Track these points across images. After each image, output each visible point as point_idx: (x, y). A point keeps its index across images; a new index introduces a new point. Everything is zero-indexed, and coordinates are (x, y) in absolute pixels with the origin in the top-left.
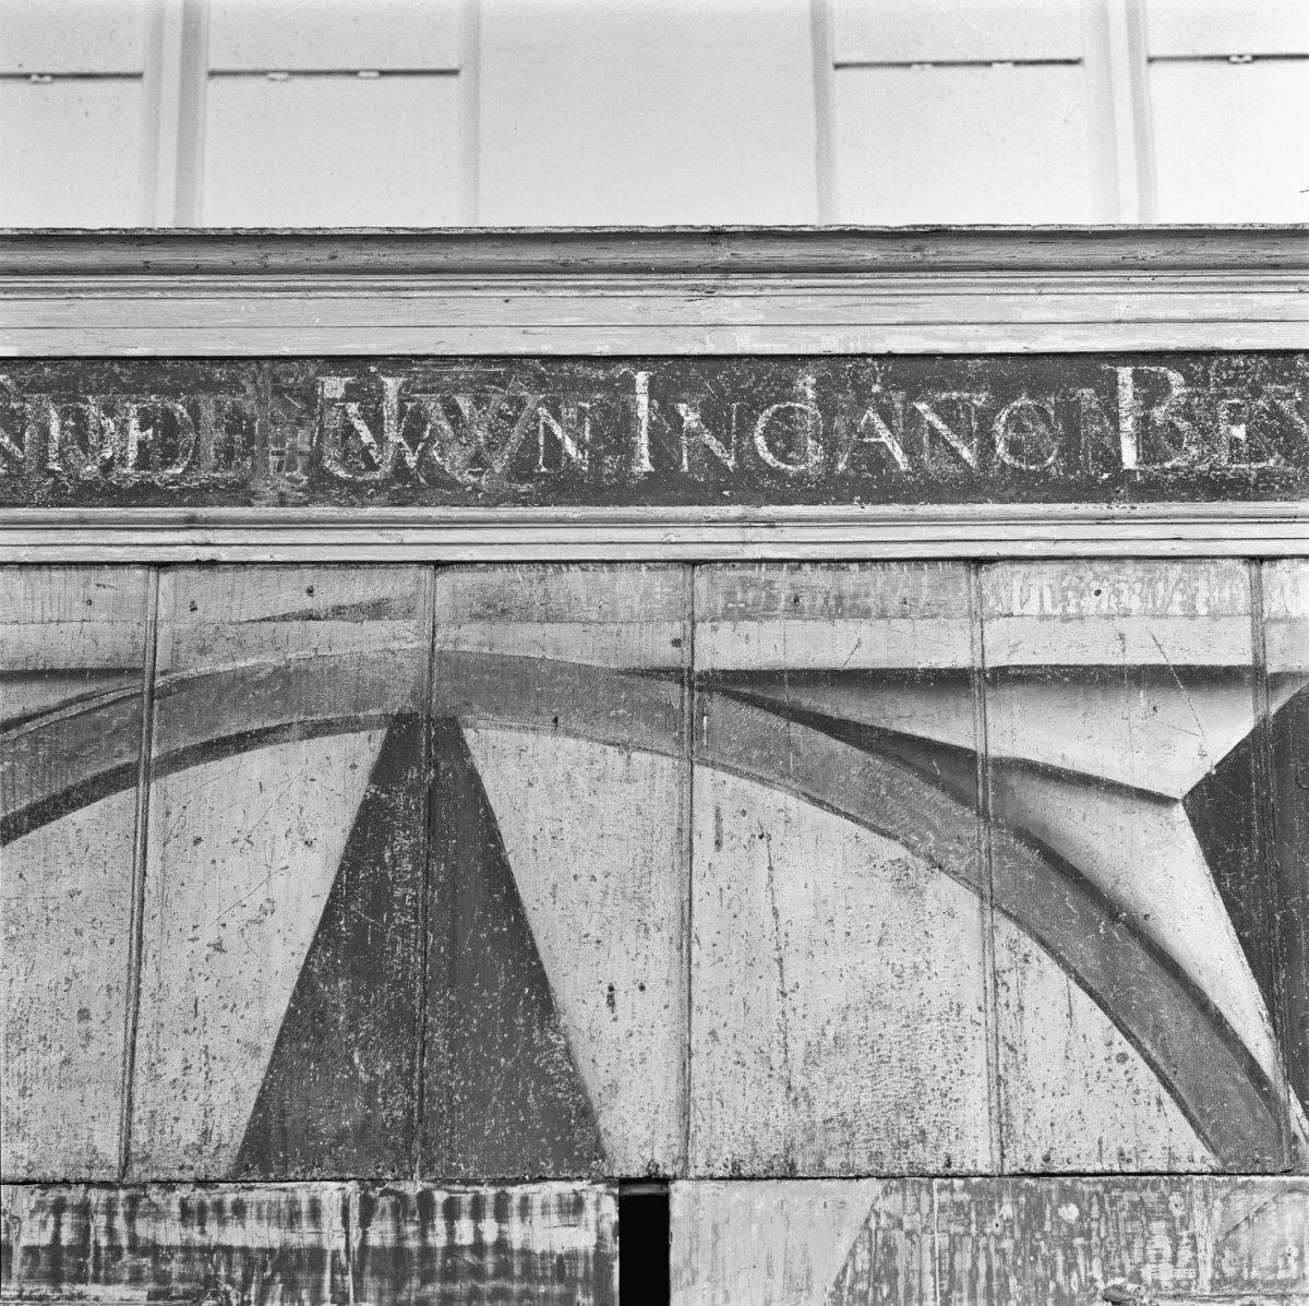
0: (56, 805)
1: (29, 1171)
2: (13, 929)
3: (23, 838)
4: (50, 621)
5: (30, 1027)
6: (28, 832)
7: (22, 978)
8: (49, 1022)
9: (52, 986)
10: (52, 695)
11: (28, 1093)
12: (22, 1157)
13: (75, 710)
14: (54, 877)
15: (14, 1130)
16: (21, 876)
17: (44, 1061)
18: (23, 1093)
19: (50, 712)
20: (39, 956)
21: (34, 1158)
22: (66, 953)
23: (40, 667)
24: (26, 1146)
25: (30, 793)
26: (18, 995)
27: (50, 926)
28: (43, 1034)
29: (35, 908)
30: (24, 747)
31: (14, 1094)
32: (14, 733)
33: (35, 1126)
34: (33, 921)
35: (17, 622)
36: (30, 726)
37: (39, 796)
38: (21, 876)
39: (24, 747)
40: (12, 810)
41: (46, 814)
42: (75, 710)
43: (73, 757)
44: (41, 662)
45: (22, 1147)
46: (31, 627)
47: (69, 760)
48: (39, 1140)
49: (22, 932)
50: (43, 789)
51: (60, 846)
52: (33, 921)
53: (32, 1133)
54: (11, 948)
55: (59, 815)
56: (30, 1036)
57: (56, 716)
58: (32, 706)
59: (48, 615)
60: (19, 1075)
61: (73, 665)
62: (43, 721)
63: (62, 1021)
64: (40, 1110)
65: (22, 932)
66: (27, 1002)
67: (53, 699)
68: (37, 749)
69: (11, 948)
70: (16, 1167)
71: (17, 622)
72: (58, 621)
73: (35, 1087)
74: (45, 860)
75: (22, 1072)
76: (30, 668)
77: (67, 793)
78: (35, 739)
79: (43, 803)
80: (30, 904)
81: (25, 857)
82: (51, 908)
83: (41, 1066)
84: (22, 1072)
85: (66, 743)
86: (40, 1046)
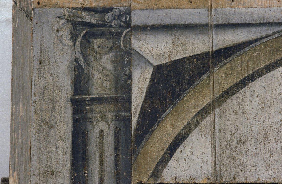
0: (273, 66)
1: (274, 180)
2: (263, 105)
3: (264, 76)
4: (267, 7)
5: (271, 135)
6: (265, 74)
7: (267, 120)
8: (276, 134)
9: (277, 122)
10: (270, 31)
11: (272, 156)
12: (271, 176)
13: (277, 35)
14: (275, 88)
15: (268, 167)
16: (264, 88)
17: (276, 146)
18: (270, 155)
19: (269, 36)
20: (272, 113)
21: (275, 176)
22: (280, 112)
23: (265, 22)
24: (273, 172)
25: (265, 62)
26: (266, 125)
27: (275, 104)
28: (275, 137)
29: (269, 98)
30: (262, 47)
31: (268, 156)
32: (259, 43)
33: (275, 166)
34: (269, 102)
35: (257, 7)
36: (264, 41)
37: (268, 63)
38: (264, 88)
39: (262, 47)
40: (260, 67)
41: (271, 69)
42: (277, 35)
43: (277, 51)
44: (265, 20)
45: (271, 173)
46: (261, 9)
47: (276, 51)
48: (276, 170)
49: (266, 106)
50: (269, 61)
51: (276, 79)
52: (269, 102)
53: (274, 168)
54: (263, 111)
55: (275, 69)
56: (271, 138)
57: (271, 37)
58: (264, 34)
59: (266, 5)
60: (269, 150)
61: (275, 21)
62: (267, 39)
63: (280, 134)
64: (276, 161)
65: (266, 106)
66: (269, 128)
67: (270, 32)
68: (266, 48)
69: (263, 111)
70: (270, 179)
71: (257, 7)
72: (270, 7)
73: (274, 154)
74: (271, 83)
75: (269, 149)
76: (262, 22)
77: (276, 62)
78: (266, 46)
79: (269, 65)
80: (268, 97)
81: (265, 82)
82: (274, 98)
83: (275, 148)
84: (269, 149)
85: (275, 46)
86: (274, 141)
